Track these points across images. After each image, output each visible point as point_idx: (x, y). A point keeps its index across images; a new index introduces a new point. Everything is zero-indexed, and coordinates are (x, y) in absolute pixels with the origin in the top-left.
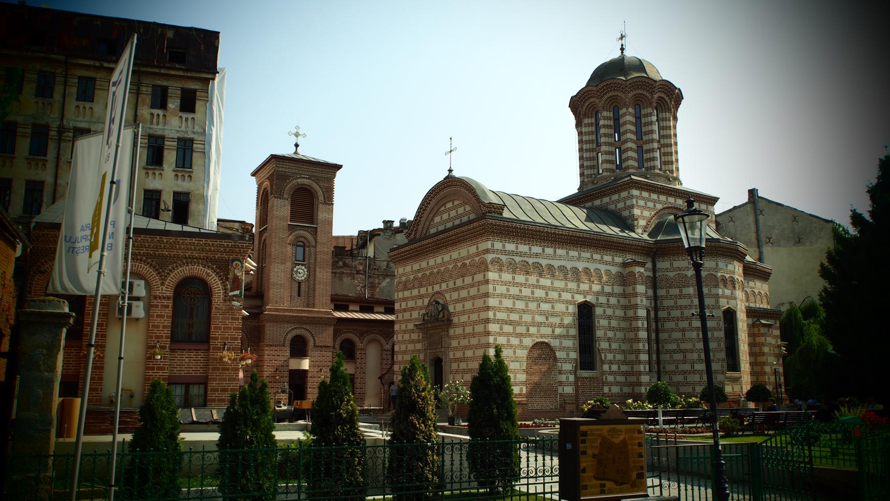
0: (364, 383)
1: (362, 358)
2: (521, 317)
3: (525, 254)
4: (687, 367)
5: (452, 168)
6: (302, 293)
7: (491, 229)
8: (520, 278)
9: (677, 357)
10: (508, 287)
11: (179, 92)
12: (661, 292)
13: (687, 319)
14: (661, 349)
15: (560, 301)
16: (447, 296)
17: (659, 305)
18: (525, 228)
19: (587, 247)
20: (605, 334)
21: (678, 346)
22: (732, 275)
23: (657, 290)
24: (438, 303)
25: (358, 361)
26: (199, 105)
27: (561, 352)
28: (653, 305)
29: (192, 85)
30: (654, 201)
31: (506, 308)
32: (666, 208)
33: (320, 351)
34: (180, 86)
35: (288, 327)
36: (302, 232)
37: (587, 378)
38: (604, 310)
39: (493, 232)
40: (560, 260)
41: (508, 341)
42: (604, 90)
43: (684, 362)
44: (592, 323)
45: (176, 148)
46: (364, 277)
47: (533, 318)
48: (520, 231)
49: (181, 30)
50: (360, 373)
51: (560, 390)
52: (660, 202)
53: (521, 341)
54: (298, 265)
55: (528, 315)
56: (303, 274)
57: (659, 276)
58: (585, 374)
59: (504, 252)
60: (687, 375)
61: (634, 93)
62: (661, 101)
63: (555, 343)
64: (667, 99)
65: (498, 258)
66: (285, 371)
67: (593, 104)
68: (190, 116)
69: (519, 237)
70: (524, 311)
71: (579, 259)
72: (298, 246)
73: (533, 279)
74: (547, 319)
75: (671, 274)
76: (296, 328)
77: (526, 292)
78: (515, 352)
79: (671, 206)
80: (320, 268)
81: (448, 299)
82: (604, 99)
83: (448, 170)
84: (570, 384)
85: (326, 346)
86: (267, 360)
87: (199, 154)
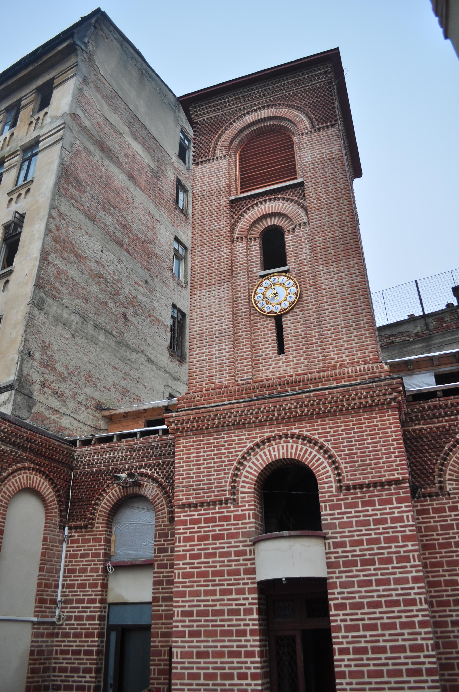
6: (289, 342)
33: (365, 504)
66: (240, 592)
76: (269, 440)
85: (382, 484)
86: (184, 557)
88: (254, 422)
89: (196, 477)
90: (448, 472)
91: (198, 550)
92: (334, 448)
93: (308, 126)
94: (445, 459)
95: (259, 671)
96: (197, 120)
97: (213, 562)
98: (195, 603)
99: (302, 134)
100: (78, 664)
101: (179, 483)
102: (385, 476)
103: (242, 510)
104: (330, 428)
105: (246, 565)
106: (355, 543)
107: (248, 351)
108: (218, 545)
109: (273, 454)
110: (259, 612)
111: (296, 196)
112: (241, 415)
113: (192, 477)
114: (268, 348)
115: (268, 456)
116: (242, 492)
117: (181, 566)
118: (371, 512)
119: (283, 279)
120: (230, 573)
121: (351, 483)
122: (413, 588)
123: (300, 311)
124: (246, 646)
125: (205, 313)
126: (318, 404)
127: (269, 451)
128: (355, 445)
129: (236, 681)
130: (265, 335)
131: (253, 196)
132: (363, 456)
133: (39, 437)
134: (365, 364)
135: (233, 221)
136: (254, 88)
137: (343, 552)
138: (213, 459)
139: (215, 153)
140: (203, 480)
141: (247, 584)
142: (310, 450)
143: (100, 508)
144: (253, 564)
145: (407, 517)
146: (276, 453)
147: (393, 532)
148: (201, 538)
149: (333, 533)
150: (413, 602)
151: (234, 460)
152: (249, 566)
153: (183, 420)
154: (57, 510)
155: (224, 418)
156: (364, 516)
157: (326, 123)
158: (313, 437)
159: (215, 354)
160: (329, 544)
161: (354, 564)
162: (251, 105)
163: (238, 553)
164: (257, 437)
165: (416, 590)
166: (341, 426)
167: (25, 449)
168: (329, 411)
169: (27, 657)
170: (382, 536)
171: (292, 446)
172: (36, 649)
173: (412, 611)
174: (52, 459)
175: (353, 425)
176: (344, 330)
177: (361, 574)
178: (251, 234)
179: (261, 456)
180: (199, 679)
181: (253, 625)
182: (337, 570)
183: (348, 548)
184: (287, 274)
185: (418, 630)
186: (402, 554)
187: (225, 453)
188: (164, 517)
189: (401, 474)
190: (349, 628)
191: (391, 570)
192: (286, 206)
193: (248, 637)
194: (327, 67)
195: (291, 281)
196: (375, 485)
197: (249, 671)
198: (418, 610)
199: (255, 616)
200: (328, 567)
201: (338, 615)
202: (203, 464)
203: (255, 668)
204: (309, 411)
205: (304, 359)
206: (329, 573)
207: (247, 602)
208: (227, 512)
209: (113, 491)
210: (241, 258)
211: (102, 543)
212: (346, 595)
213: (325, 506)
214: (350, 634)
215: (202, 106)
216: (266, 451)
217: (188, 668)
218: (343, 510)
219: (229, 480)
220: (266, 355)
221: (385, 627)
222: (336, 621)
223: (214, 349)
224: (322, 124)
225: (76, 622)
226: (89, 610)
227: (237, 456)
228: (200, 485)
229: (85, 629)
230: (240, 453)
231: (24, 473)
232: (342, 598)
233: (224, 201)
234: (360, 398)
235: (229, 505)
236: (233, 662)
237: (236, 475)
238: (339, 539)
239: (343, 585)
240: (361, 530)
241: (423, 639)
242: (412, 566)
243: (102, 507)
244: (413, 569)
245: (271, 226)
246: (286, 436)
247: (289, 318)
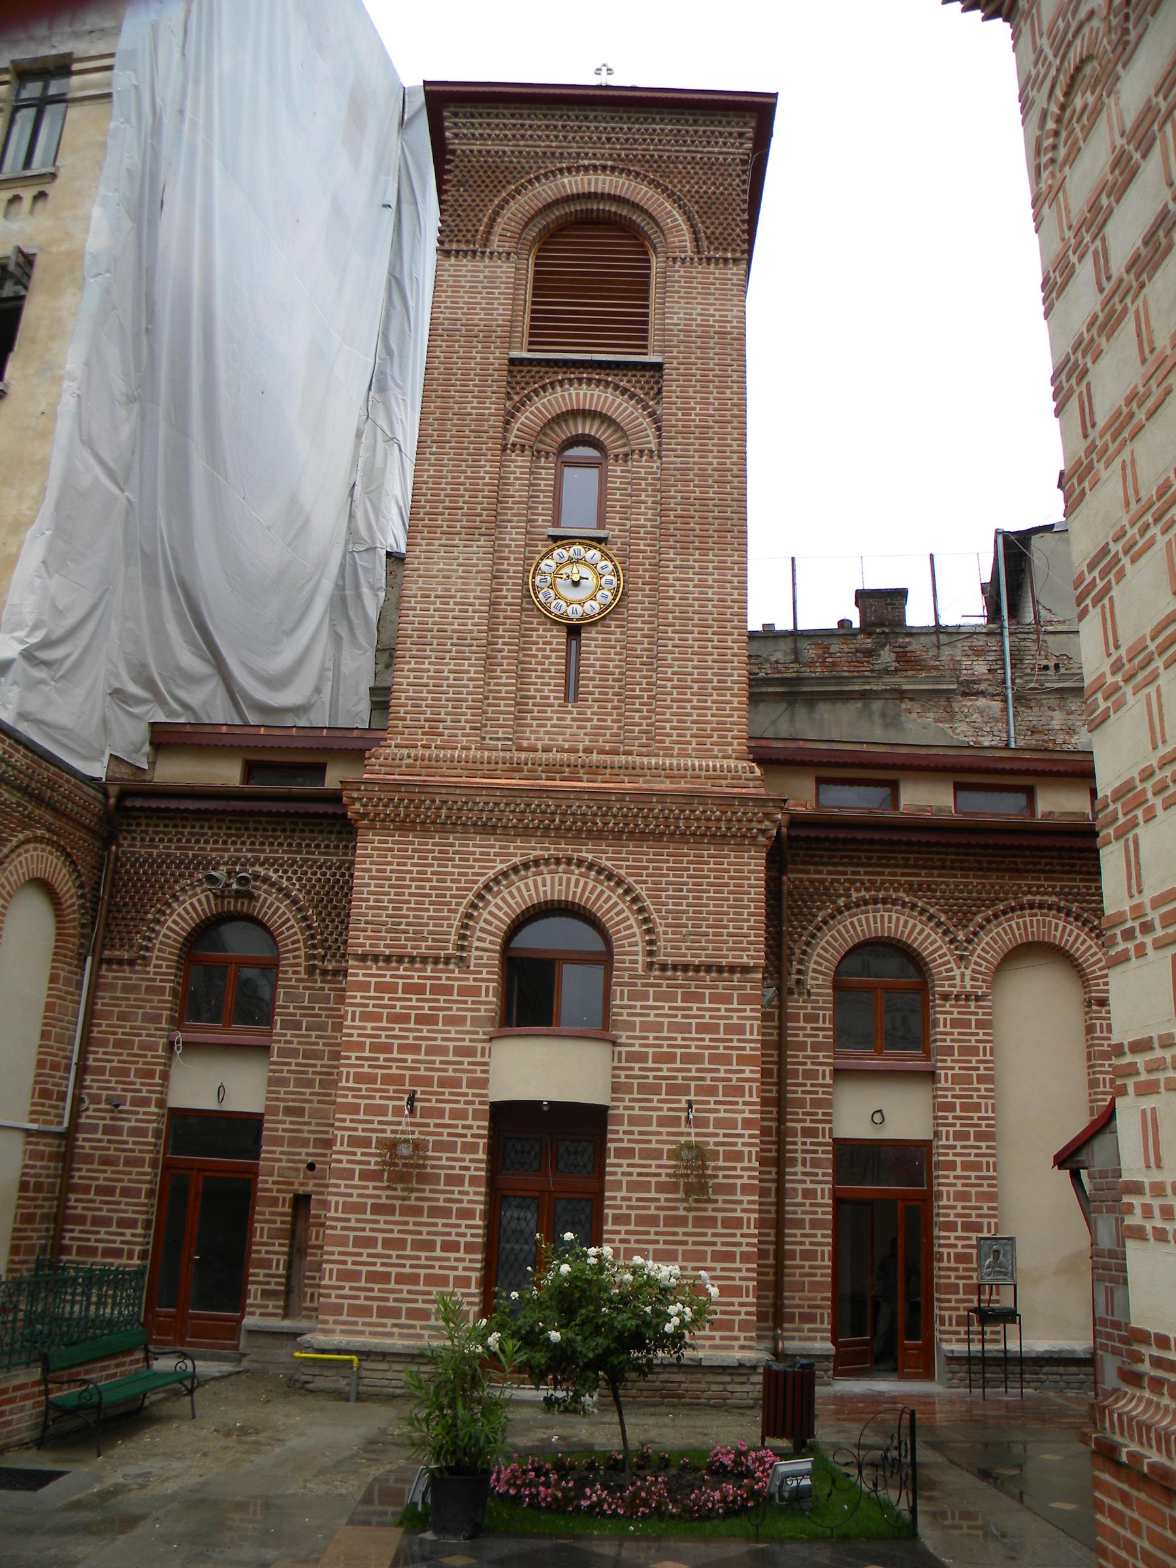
0: (992, 1197)
1: (974, 1051)
25: (948, 1067)
33: (687, 997)
35: (485, 859)
46: (996, 705)
50: (959, 1136)
56: (566, 570)
76: (536, 863)
85: (720, 969)
86: (360, 1046)
88: (514, 827)
89: (394, 909)
90: (815, 958)
91: (387, 1037)
92: (650, 897)
93: (688, 244)
94: (813, 936)
95: (480, 1240)
96: (455, 144)
97: (414, 1061)
98: (375, 1126)
99: (674, 259)
100: (109, 1210)
101: (359, 914)
102: (727, 957)
103: (475, 980)
104: (649, 861)
105: (474, 1071)
106: (661, 1058)
107: (511, 685)
108: (425, 1034)
109: (541, 889)
110: (491, 1149)
111: (642, 388)
112: (492, 811)
113: (386, 908)
114: (548, 684)
115: (533, 892)
116: (477, 949)
117: (353, 1061)
118: (694, 1012)
119: (593, 554)
120: (443, 1083)
121: (670, 960)
122: (741, 1136)
123: (617, 626)
124: (461, 1201)
125: (435, 590)
126: (636, 816)
127: (535, 882)
128: (686, 898)
129: (438, 1253)
130: (544, 657)
131: (556, 363)
132: (697, 917)
133: (68, 782)
134: (724, 757)
135: (508, 403)
136: (592, 115)
137: (641, 1069)
138: (430, 880)
139: (487, 239)
140: (407, 917)
141: (472, 1103)
142: (608, 892)
143: (164, 930)
144: (486, 1072)
145: (752, 1026)
146: (548, 888)
147: (725, 1048)
148: (394, 1018)
149: (628, 1037)
151: (470, 889)
152: (479, 1075)
153: (380, 799)
154: (76, 924)
155: (460, 810)
156: (683, 1017)
157: (725, 250)
158: (616, 871)
159: (447, 679)
160: (620, 1053)
161: (656, 1090)
162: (578, 154)
163: (459, 1051)
164: (515, 855)
165: (746, 1140)
166: (667, 861)
167: (39, 800)
168: (652, 832)
169: (14, 1192)
170: (707, 1052)
171: (577, 882)
172: (33, 1180)
173: (734, 1169)
174: (79, 823)
175: (689, 862)
176: (696, 686)
177: (665, 1106)
178: (541, 442)
179: (519, 889)
180: (375, 1247)
181: (476, 1169)
182: (627, 1097)
183: (650, 1065)
184: (602, 546)
185: (739, 1197)
186: (734, 1083)
187: (452, 874)
188: (297, 965)
189: (753, 957)
190: (632, 1186)
191: (712, 1106)
192: (620, 405)
193: (466, 1188)
194: (745, 125)
195: (608, 563)
196: (708, 968)
197: (462, 1240)
198: (743, 1169)
199: (482, 1155)
200: (614, 1090)
201: (620, 1166)
202: (410, 887)
203: (473, 1235)
204: (616, 824)
205: (613, 721)
206: (613, 1100)
207: (469, 1132)
208: (448, 979)
209: (194, 900)
210: (517, 489)
211: (167, 997)
212: (636, 1137)
213: (622, 992)
214: (635, 1195)
215: (472, 116)
216: (530, 881)
217: (355, 1229)
218: (651, 1003)
219: (456, 923)
220: (542, 698)
222: (615, 1173)
223: (446, 668)
224: (716, 249)
225: (106, 1137)
226: (134, 1117)
227: (476, 882)
228: (400, 924)
229: (124, 1150)
230: (482, 879)
231: (35, 849)
232: (630, 1141)
233: (497, 357)
234: (709, 819)
235: (451, 967)
236: (407, 1223)
237: (469, 916)
238: (637, 1049)
239: (633, 1121)
240: (675, 1039)
241: (744, 1211)
242: (745, 1103)
243: (169, 928)
244: (747, 1108)
245: (583, 435)
246: (569, 861)
247: (594, 635)
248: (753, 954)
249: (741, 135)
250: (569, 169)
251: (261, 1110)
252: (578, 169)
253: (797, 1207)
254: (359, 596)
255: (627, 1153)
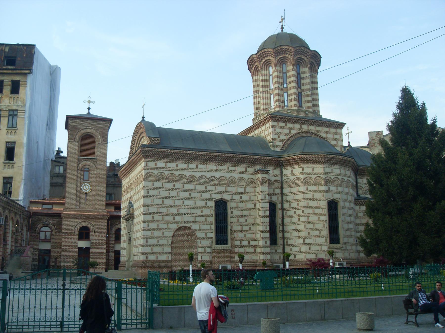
2: (168, 210)
3: (173, 169)
4: (301, 241)
5: (144, 116)
6: (87, 201)
7: (145, 154)
8: (168, 185)
9: (296, 234)
10: (159, 191)
11: (10, 83)
12: (285, 191)
13: (301, 208)
14: (285, 229)
15: (200, 199)
16: (133, 198)
17: (284, 199)
18: (172, 152)
19: (223, 163)
20: (238, 220)
21: (296, 227)
22: (336, 176)
23: (283, 189)
24: (130, 203)
26: (21, 89)
27: (200, 233)
28: (280, 199)
29: (17, 78)
30: (290, 129)
31: (157, 204)
32: (300, 132)
34: (11, 79)
36: (87, 162)
37: (221, 250)
38: (237, 205)
39: (147, 156)
40: (201, 172)
41: (158, 226)
42: (261, 56)
43: (299, 238)
44: (227, 213)
45: (8, 116)
47: (178, 211)
48: (168, 154)
49: (13, 46)
51: (199, 258)
52: (294, 129)
53: (168, 226)
54: (85, 182)
55: (174, 209)
57: (285, 179)
58: (220, 247)
59: (157, 168)
60: (300, 247)
61: (280, 57)
62: (303, 61)
63: (195, 227)
64: (305, 58)
65: (152, 172)
66: (75, 249)
67: (257, 66)
68: (16, 96)
69: (168, 158)
70: (171, 206)
71: (216, 171)
72: (84, 171)
73: (178, 186)
74: (190, 211)
75: (292, 178)
77: (173, 194)
78: (163, 234)
79: (304, 131)
80: (99, 184)
81: (134, 201)
82: (262, 63)
83: (142, 118)
84: (207, 254)
86: (64, 242)
87: (21, 118)
106: (96, 242)
119: (88, 184)
150: (104, 252)
196: (101, 233)
210: (79, 176)
221: (99, 256)
233: (76, 158)
239: (93, 249)
248: (105, 231)
249: (108, 124)
250: (85, 128)
251: (50, 249)
252: (86, 128)
253: (110, 258)
254: (47, 167)
255: (92, 252)
